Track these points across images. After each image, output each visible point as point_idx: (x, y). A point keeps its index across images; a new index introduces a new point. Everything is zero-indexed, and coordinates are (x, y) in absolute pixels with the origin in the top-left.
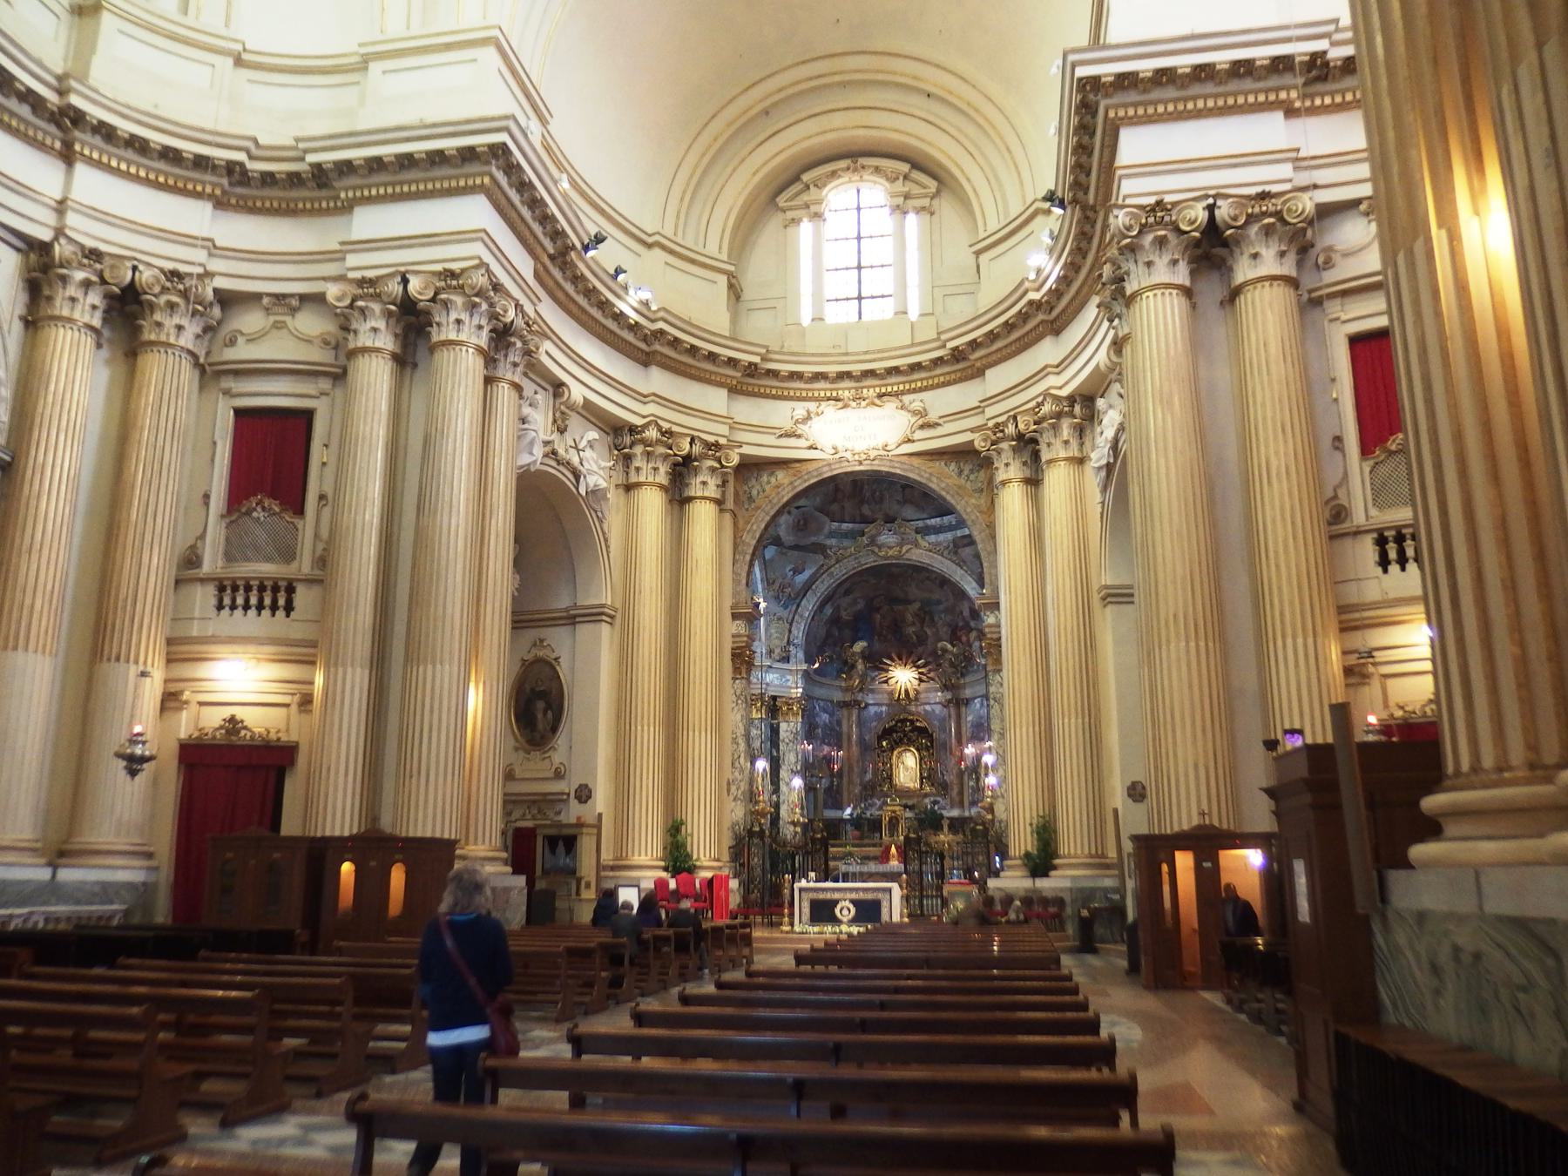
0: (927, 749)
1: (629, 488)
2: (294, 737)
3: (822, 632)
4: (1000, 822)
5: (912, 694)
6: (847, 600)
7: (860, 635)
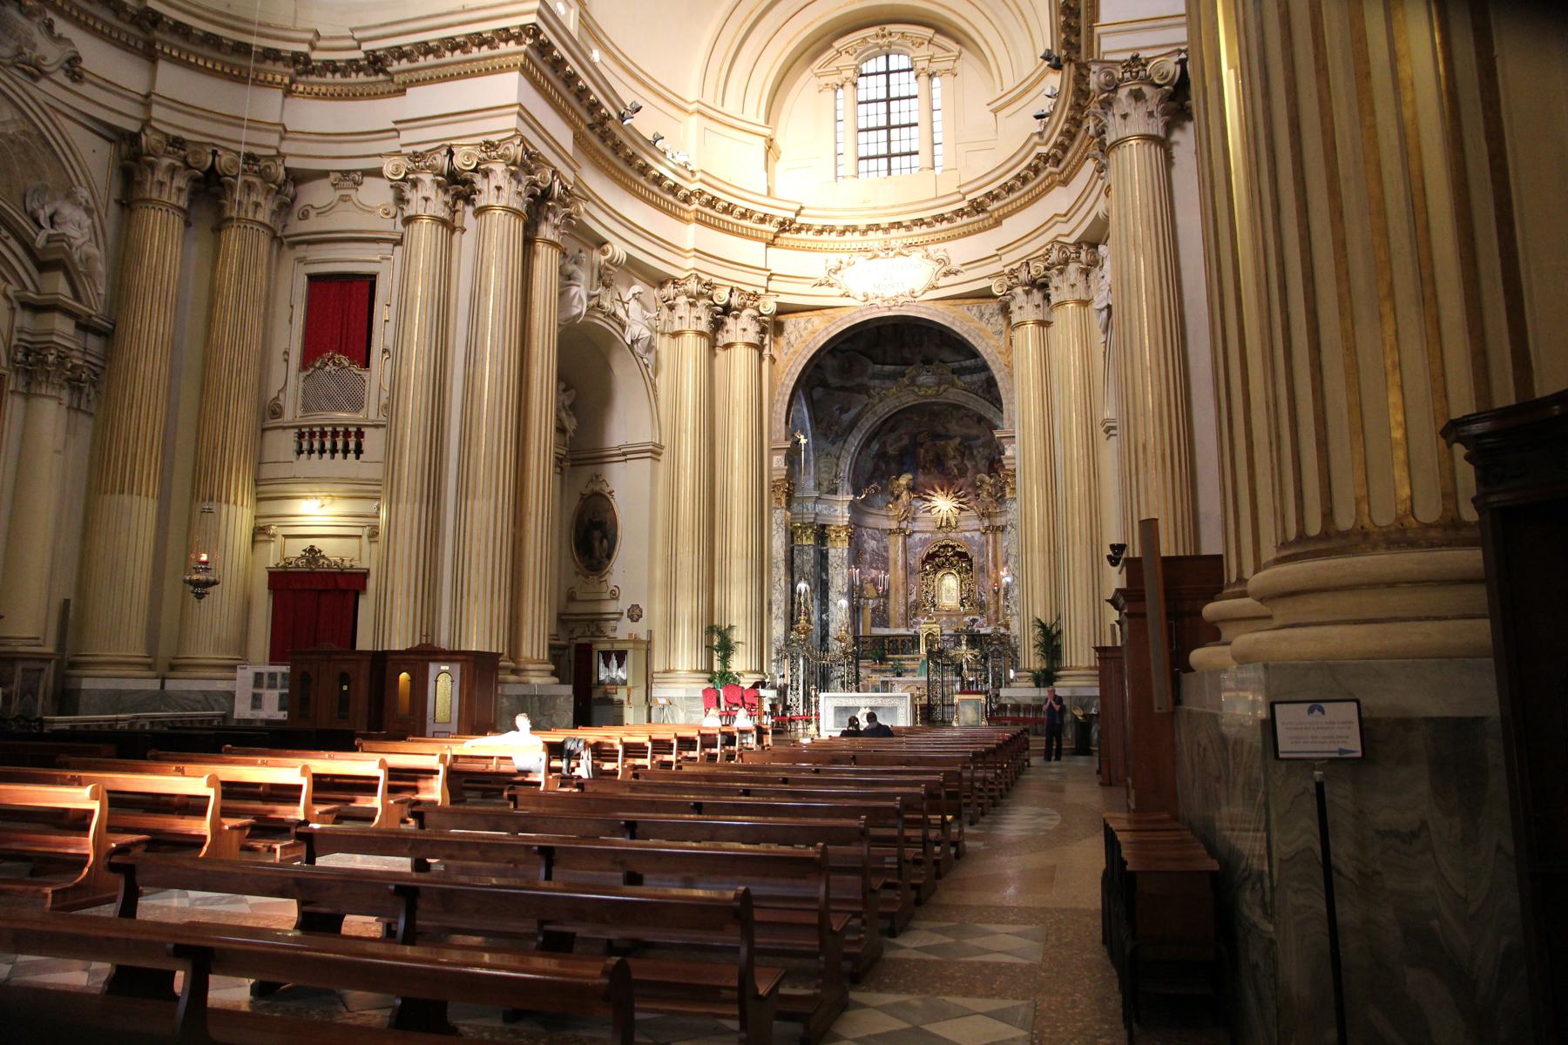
0: (967, 572)
1: (676, 335)
2: (365, 565)
3: (869, 465)
4: (1015, 637)
5: (953, 524)
6: (894, 436)
7: (905, 468)
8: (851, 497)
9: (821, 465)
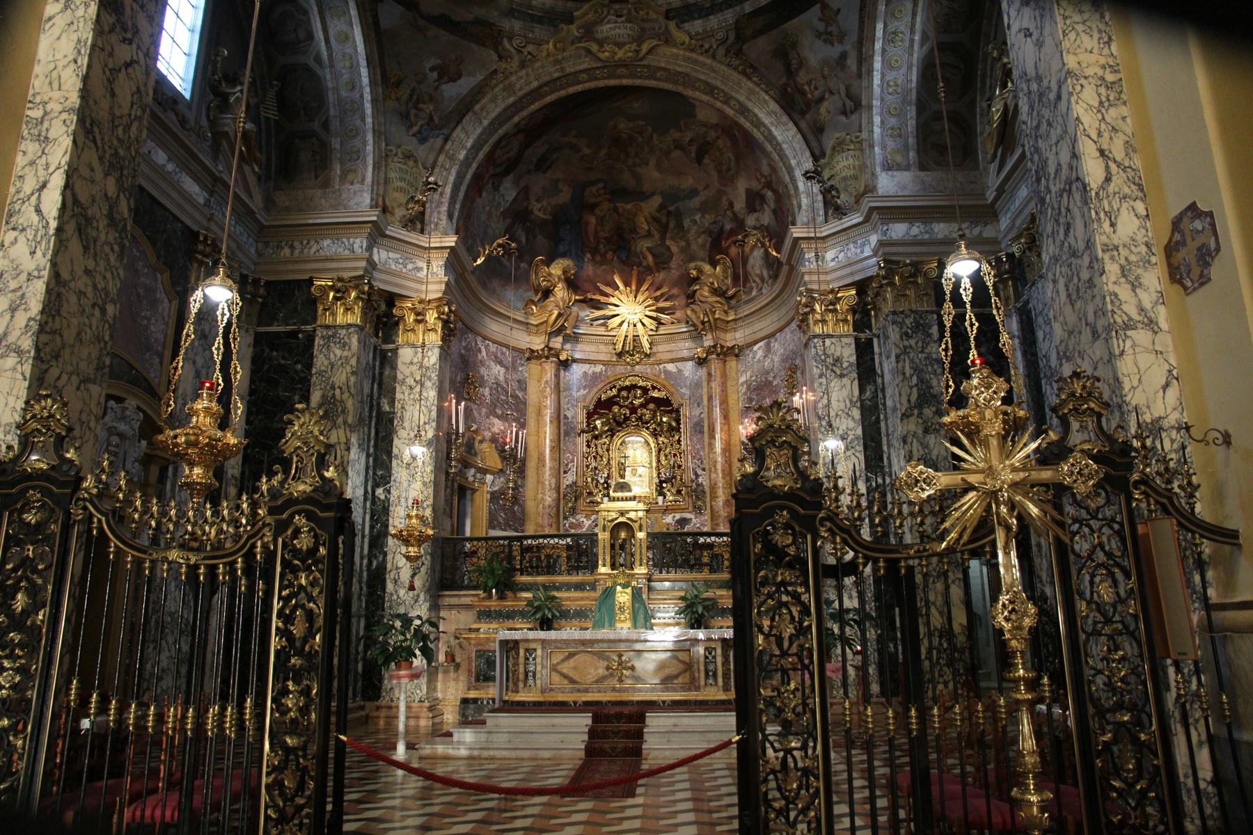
7: (561, 248)
8: (451, 241)
9: (392, 175)
